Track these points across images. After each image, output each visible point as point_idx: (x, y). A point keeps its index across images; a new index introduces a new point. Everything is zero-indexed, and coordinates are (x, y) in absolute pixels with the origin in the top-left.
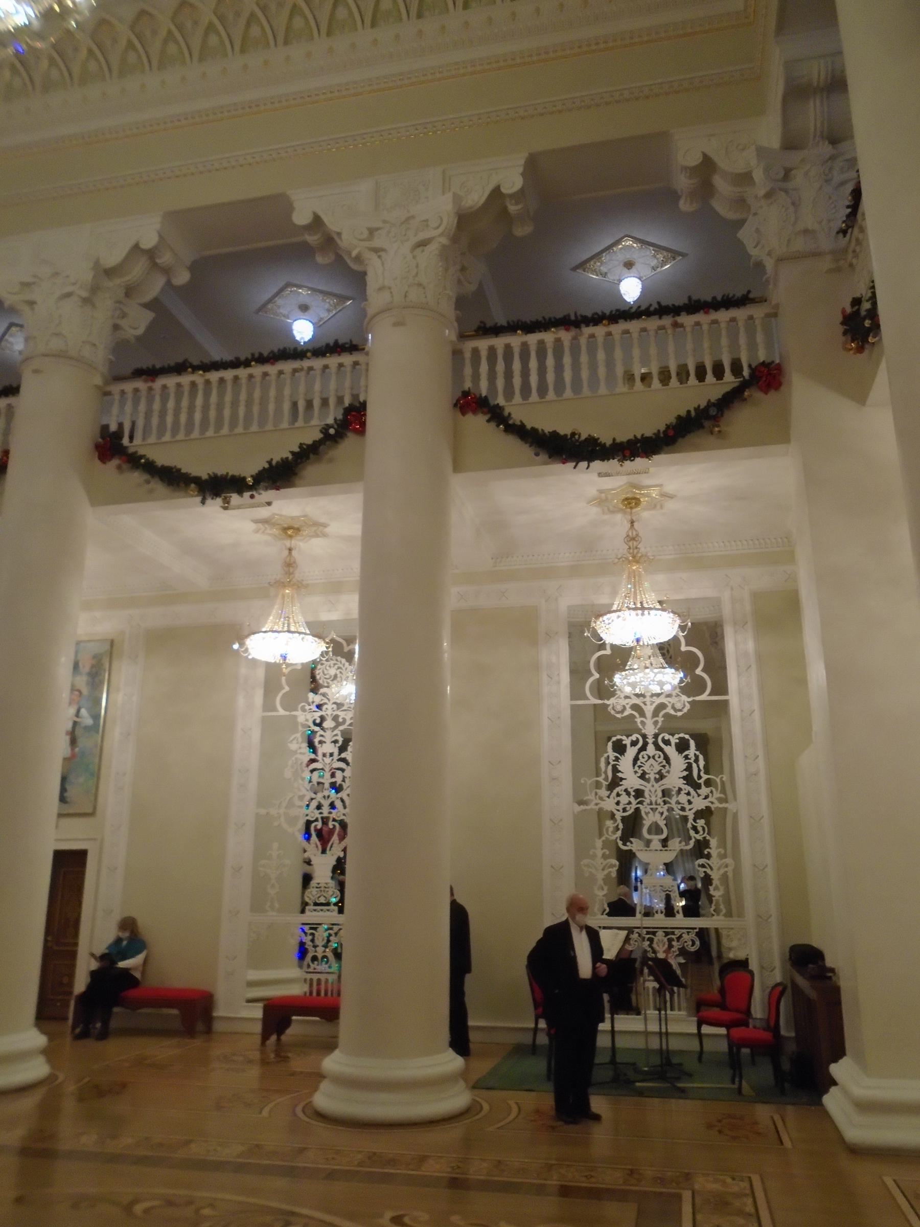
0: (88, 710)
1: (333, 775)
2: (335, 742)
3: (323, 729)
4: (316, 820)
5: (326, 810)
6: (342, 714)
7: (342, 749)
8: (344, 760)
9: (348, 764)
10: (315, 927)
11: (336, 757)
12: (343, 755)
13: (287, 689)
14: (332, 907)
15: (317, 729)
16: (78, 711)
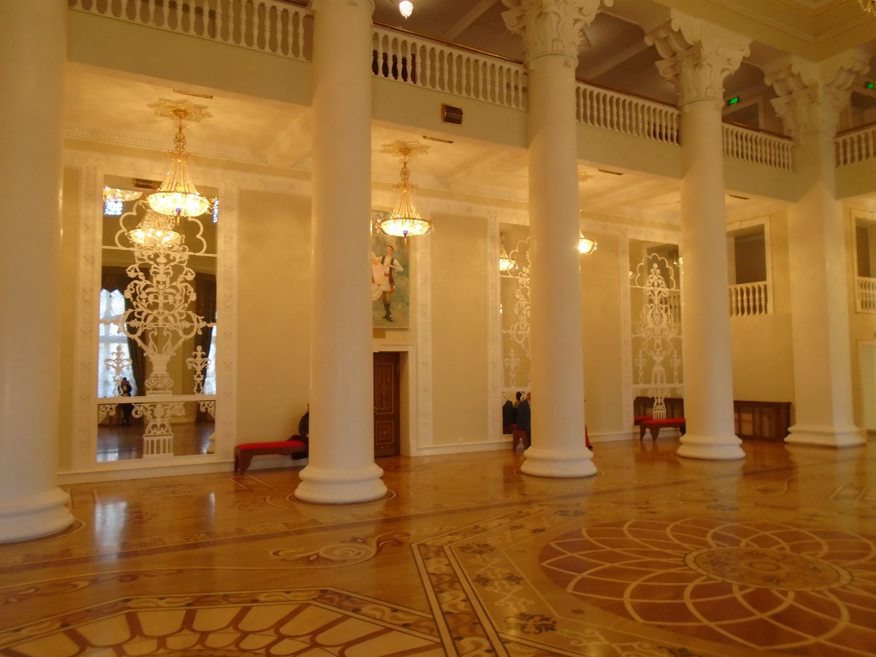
0: (399, 261)
1: (166, 298)
2: (167, 274)
3: (157, 264)
4: (153, 329)
5: (161, 323)
6: (173, 254)
7: (173, 279)
8: (175, 288)
9: (177, 290)
10: (154, 405)
11: (168, 284)
12: (174, 284)
13: (199, 236)
14: (168, 391)
15: (151, 262)
16: (392, 261)
